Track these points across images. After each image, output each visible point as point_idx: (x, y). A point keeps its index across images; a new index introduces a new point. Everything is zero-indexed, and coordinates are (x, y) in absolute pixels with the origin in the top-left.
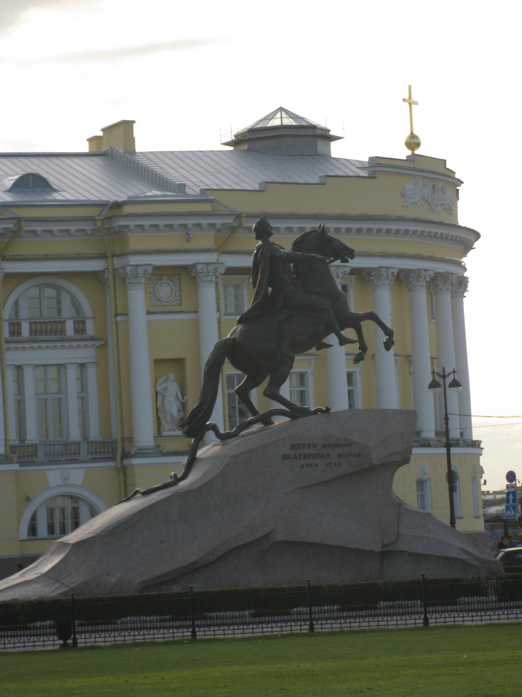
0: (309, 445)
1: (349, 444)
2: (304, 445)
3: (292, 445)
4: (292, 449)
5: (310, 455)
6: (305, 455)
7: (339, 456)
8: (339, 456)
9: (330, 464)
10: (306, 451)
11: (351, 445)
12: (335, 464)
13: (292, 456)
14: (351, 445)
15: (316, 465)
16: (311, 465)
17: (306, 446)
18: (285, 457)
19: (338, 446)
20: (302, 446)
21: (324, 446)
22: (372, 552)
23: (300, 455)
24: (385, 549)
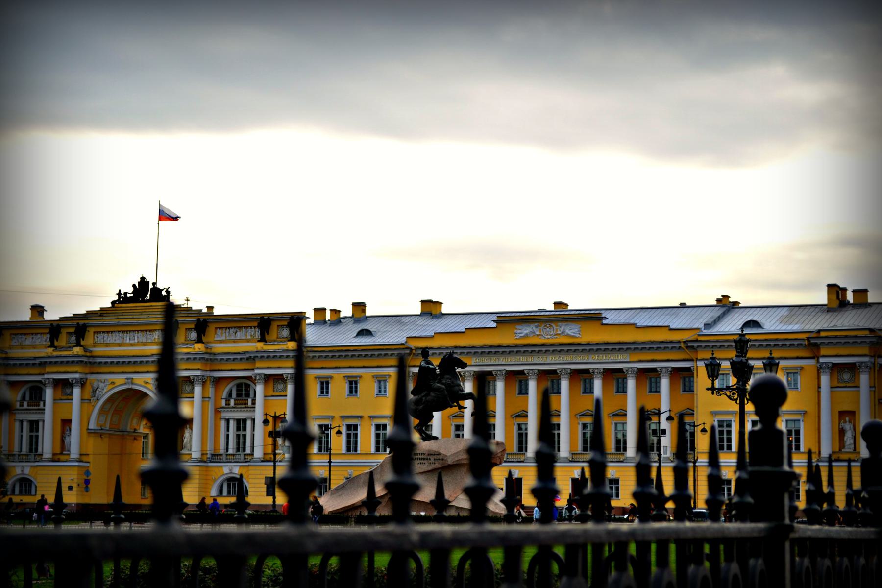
1: (439, 454)
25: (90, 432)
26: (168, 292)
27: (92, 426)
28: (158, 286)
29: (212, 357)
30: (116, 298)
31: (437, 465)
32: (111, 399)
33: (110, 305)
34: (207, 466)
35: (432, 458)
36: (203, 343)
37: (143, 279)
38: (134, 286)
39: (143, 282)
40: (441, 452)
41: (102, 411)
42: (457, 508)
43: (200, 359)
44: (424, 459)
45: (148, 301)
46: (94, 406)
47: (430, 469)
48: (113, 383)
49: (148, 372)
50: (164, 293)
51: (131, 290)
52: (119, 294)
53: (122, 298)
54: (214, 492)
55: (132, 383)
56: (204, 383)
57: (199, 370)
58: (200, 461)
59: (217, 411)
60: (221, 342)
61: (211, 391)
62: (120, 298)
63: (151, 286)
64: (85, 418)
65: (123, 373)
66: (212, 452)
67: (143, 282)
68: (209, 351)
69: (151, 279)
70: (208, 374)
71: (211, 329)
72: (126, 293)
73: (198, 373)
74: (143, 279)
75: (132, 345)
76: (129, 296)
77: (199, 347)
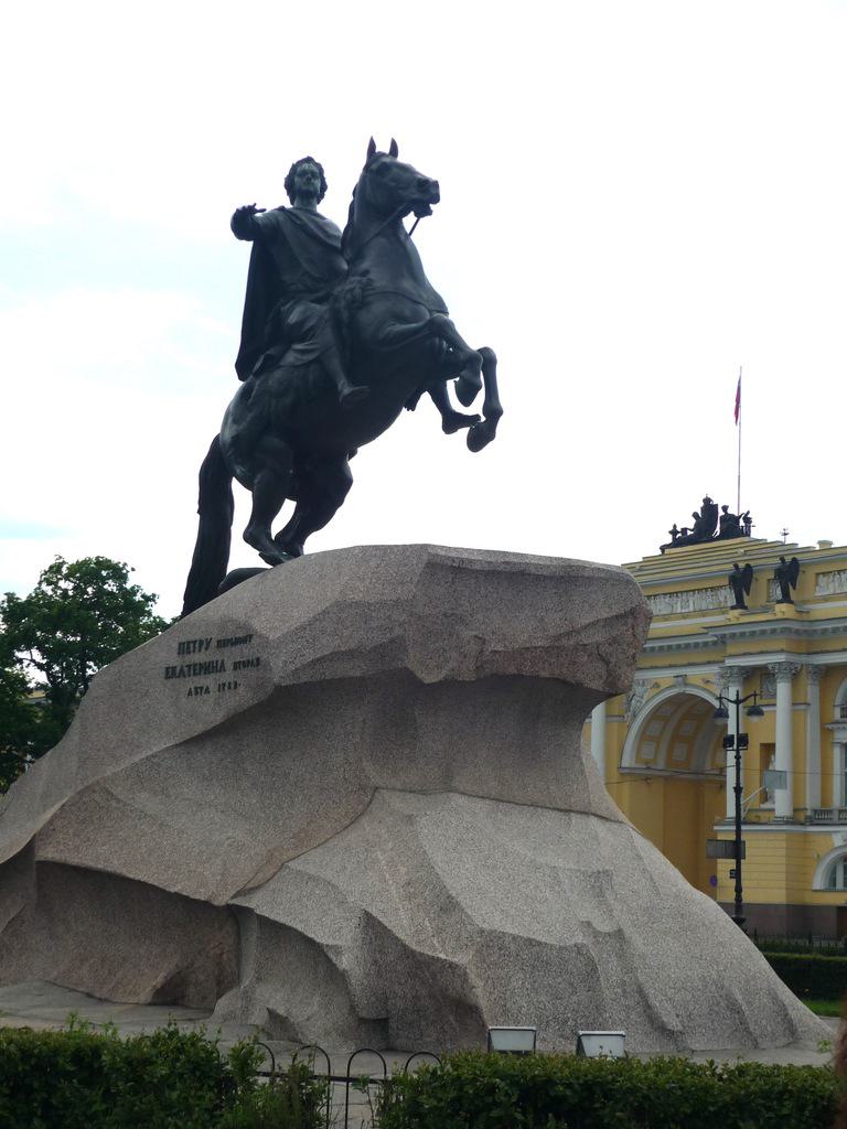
0: (201, 642)
3: (180, 644)
4: (179, 653)
6: (195, 665)
8: (236, 666)
9: (224, 685)
10: (199, 657)
12: (229, 688)
14: (251, 636)
15: (207, 691)
16: (202, 688)
17: (197, 645)
18: (171, 673)
20: (192, 645)
21: (222, 644)
22: (206, 905)
23: (189, 666)
24: (235, 901)
25: (626, 774)
26: (748, 520)
27: (627, 761)
28: (732, 511)
29: (806, 627)
30: (669, 539)
31: (242, 698)
32: (656, 714)
33: (659, 552)
34: (806, 833)
35: (230, 656)
36: (792, 602)
37: (707, 501)
38: (695, 515)
39: (709, 507)
40: (258, 625)
41: (643, 736)
42: (266, 923)
43: (784, 630)
44: (207, 668)
45: (718, 538)
46: (629, 727)
47: (218, 717)
48: (657, 685)
49: (709, 663)
50: (742, 523)
51: (691, 523)
52: (674, 532)
53: (680, 539)
54: (819, 882)
55: (686, 684)
56: (795, 676)
57: (782, 651)
58: (793, 823)
59: (826, 732)
60: (826, 599)
61: (811, 691)
62: (674, 539)
63: (721, 513)
64: (613, 749)
65: (671, 666)
66: (818, 805)
67: (709, 507)
68: (805, 617)
69: (718, 501)
70: (804, 659)
71: (806, 578)
72: (684, 530)
73: (781, 658)
74: (707, 501)
75: (684, 616)
76: (689, 533)
77: (783, 610)
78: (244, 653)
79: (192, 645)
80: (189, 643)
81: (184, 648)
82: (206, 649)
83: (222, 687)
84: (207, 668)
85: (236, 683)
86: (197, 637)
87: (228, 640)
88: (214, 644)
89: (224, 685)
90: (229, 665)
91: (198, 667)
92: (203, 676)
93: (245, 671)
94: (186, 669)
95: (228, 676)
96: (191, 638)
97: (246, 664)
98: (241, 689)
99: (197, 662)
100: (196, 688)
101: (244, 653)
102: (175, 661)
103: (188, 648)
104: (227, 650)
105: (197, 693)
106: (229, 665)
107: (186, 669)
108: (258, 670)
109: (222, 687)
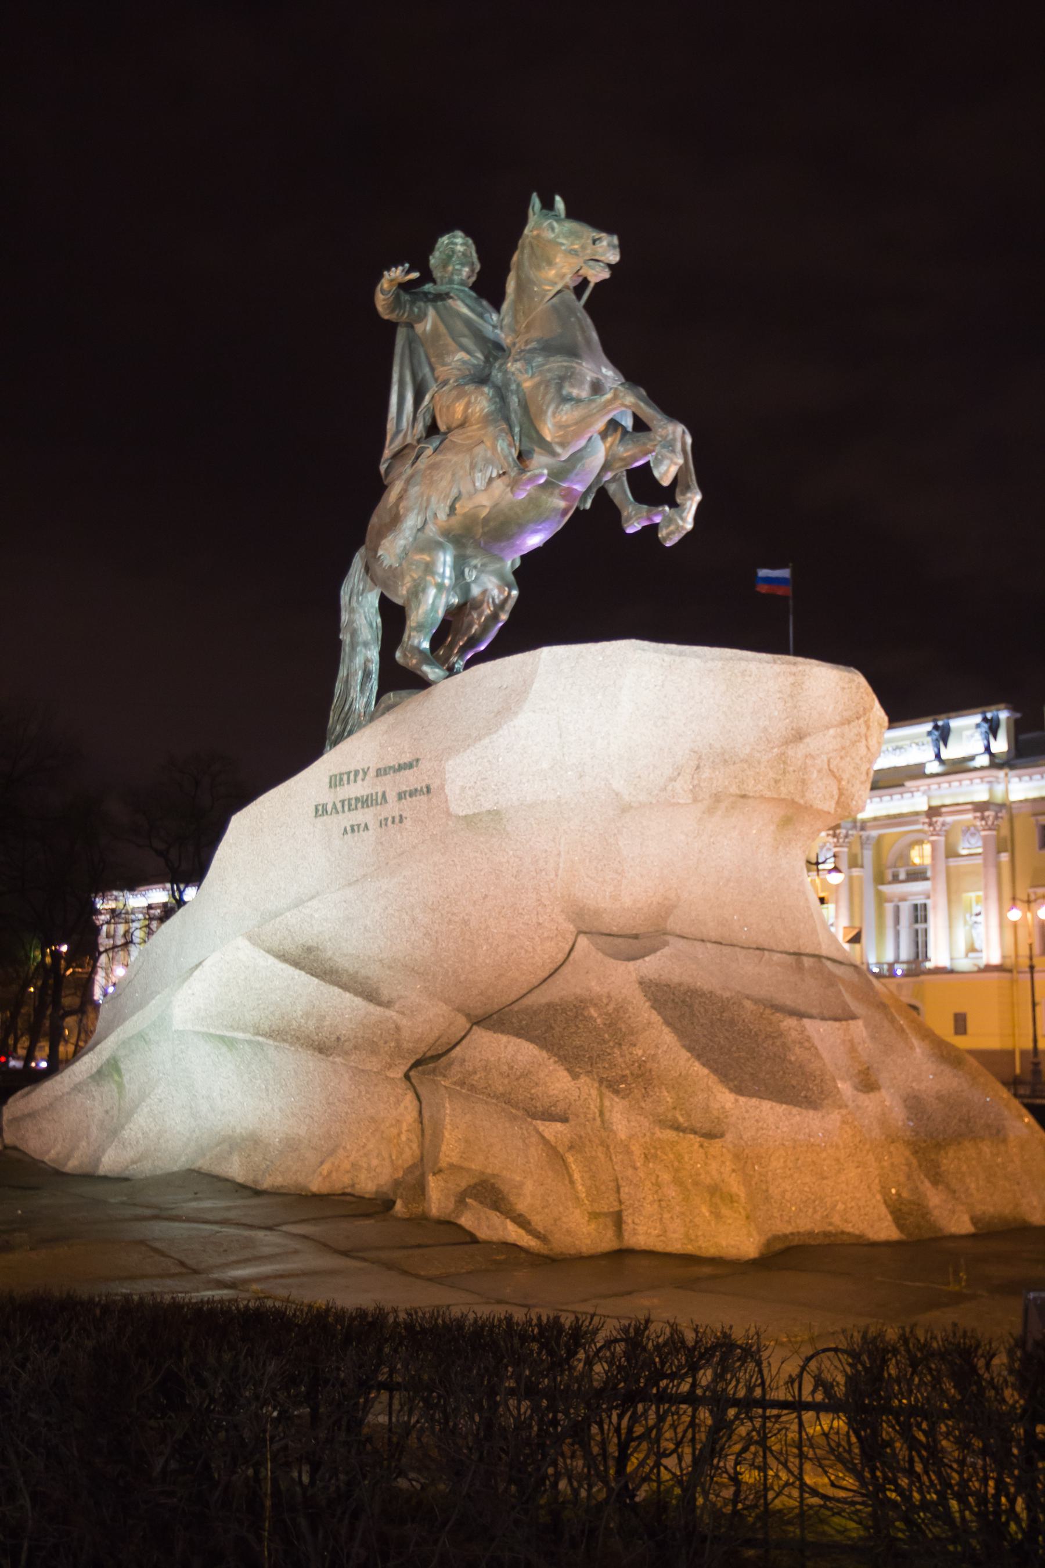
0: (357, 773)
2: (349, 773)
4: (331, 787)
5: (357, 799)
6: (350, 800)
7: (401, 796)
9: (386, 819)
11: (418, 760)
12: (393, 822)
13: (329, 808)
14: (418, 760)
15: (366, 827)
16: (359, 826)
18: (321, 811)
19: (401, 768)
20: (345, 777)
23: (343, 802)
44: (365, 802)
78: (409, 780)
79: (345, 777)
80: (341, 774)
81: (335, 781)
82: (363, 780)
83: (383, 823)
84: (365, 802)
85: (401, 816)
86: (352, 768)
87: (390, 768)
88: (372, 773)
89: (386, 819)
90: (391, 796)
91: (353, 802)
92: (360, 811)
93: (408, 802)
94: (339, 806)
95: (392, 808)
96: (344, 769)
97: (413, 793)
98: (408, 823)
99: (353, 796)
100: (352, 827)
101: (409, 780)
102: (327, 797)
103: (341, 780)
104: (387, 779)
105: (353, 830)
106: (391, 796)
107: (339, 806)
108: (430, 800)
109: (383, 823)
